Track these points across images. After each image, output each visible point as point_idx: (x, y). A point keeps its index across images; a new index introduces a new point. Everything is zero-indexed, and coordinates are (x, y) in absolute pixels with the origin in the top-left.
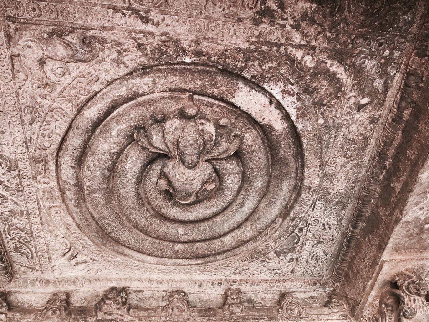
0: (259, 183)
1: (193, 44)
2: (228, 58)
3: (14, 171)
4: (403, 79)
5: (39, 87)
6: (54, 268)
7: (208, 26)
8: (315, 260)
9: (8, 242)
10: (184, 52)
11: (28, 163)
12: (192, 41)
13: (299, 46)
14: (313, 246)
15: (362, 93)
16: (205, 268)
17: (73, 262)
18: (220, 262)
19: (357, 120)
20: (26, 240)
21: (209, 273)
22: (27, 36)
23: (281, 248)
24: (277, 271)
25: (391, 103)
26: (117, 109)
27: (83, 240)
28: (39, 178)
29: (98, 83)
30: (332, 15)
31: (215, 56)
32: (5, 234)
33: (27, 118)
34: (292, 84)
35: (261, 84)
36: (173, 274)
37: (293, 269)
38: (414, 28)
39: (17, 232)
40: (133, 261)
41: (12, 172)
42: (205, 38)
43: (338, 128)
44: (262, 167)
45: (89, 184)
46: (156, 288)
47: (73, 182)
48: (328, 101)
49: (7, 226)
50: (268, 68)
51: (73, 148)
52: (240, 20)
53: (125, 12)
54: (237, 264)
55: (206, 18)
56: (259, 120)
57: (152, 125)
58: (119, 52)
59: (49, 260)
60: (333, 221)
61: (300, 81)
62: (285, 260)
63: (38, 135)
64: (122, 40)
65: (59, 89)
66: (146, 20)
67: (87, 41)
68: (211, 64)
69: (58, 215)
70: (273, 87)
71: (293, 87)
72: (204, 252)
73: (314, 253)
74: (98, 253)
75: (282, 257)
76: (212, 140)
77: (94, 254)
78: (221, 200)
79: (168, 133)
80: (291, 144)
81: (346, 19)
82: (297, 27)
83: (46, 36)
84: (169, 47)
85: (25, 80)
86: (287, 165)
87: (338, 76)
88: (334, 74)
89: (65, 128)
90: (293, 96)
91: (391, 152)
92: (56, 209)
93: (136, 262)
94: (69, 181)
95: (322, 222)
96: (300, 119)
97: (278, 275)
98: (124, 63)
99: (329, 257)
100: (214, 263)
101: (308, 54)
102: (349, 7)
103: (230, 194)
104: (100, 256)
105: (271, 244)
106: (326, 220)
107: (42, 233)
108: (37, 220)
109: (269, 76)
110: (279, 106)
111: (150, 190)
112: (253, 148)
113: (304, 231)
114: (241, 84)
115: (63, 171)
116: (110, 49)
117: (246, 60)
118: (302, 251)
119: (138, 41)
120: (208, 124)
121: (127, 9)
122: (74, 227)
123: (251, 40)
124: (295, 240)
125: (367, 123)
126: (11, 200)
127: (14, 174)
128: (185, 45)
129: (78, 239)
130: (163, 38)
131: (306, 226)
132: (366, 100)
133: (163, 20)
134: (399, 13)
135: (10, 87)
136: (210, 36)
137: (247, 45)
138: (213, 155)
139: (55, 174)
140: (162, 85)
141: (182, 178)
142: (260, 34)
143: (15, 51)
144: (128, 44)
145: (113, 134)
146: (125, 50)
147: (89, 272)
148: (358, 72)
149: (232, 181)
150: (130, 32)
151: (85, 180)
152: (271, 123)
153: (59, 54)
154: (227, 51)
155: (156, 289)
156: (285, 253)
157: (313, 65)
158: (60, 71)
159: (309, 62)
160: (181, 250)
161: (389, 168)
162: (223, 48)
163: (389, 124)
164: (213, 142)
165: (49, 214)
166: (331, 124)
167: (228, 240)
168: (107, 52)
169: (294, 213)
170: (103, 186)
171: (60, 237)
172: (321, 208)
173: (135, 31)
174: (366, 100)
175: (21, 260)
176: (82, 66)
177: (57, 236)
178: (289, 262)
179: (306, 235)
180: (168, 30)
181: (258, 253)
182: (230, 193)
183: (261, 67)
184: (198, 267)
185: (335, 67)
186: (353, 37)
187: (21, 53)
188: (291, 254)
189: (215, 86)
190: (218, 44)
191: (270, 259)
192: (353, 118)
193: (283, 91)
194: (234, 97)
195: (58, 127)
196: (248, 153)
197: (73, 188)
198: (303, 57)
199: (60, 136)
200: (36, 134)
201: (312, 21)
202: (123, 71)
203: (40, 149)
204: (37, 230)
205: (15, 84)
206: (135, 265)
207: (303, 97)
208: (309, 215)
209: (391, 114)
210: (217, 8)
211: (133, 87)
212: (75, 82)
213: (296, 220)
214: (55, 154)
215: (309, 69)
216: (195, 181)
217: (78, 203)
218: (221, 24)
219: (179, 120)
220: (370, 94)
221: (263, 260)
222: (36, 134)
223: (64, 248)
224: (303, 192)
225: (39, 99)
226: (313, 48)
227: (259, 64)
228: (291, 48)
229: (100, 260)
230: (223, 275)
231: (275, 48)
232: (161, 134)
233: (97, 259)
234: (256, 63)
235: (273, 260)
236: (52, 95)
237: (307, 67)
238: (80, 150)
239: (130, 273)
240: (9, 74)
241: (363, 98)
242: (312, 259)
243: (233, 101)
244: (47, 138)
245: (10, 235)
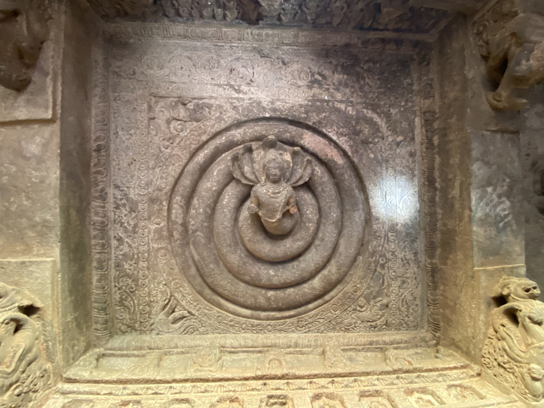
0: (334, 214)
1: (270, 104)
2: (295, 112)
3: (134, 212)
4: (421, 118)
5: (164, 140)
6: (152, 327)
7: (278, 92)
8: (405, 307)
9: (115, 292)
10: (264, 109)
11: (146, 205)
12: (269, 102)
13: (341, 102)
14: (399, 286)
15: (394, 131)
16: (298, 322)
17: (171, 317)
18: (313, 312)
19: (399, 153)
20: (131, 290)
21: (304, 328)
22: (162, 104)
23: (369, 291)
24: (372, 324)
25: (420, 138)
26: (219, 157)
27: (183, 287)
28: (152, 218)
29: (206, 135)
30: (358, 81)
31: (285, 112)
32: (115, 282)
33: (152, 163)
34: (343, 128)
35: (320, 129)
36: (267, 332)
37: (387, 321)
38: (415, 87)
39: (125, 279)
40: (228, 314)
41: (132, 213)
42: (278, 100)
43: (387, 161)
44: (334, 198)
45: (193, 222)
46: (252, 347)
47: (180, 221)
48: (373, 139)
49: (118, 273)
50: (323, 117)
51: (183, 188)
52: (299, 87)
53: (225, 87)
54: (330, 314)
55: (277, 87)
56: (323, 158)
57: (243, 154)
58: (221, 113)
59: (149, 315)
60: (410, 256)
61: (348, 125)
62: (376, 307)
63: (158, 178)
64: (223, 104)
65: (178, 140)
66: (238, 91)
67: (201, 106)
68: (283, 117)
69: (164, 258)
70: (330, 130)
71: (344, 130)
72: (295, 298)
73: (403, 297)
74: (195, 304)
75: (372, 303)
76: (290, 167)
77: (191, 306)
78: (304, 233)
79: (255, 162)
80: (353, 177)
81: (368, 84)
82: (337, 89)
83: (173, 104)
84: (254, 107)
85: (156, 135)
86: (354, 196)
87: (375, 120)
88: (371, 119)
89: (179, 171)
90: (345, 136)
92: (163, 251)
93: (230, 315)
94: (177, 220)
95: (400, 256)
96: (355, 154)
97: (373, 329)
98: (224, 120)
99: (418, 302)
100: (306, 314)
101: (349, 106)
102: (368, 76)
103: (312, 227)
104: (197, 308)
105: (358, 286)
106: (403, 255)
107: (147, 281)
108: (144, 265)
109: (325, 122)
110: (337, 145)
111: (243, 225)
112: (323, 179)
113: (386, 268)
114: (306, 131)
115: (174, 211)
116: (214, 111)
117: (306, 113)
118: (389, 294)
119: (234, 104)
120: (285, 153)
121: (226, 85)
122: (177, 270)
123: (308, 99)
124: (380, 280)
125: (407, 156)
126: (127, 242)
127: (134, 215)
128: (265, 104)
129: (178, 286)
130: (250, 101)
131: (386, 262)
132: (400, 138)
133: (249, 90)
134: (402, 79)
135: (143, 141)
136: (281, 98)
137: (306, 102)
138: (292, 182)
139: (166, 214)
140: (250, 134)
141: (268, 192)
142: (314, 94)
143: (152, 115)
144: (227, 106)
145: (215, 174)
146: (225, 111)
147: (185, 332)
148: (388, 117)
149: (311, 212)
150: (228, 99)
151: (191, 220)
152: (334, 158)
153: (181, 115)
154: (293, 107)
155: (251, 349)
156: (375, 298)
157: (354, 113)
158: (180, 127)
159: (351, 111)
160: (273, 296)
161: (441, 187)
162: (290, 105)
163: (425, 153)
164: (290, 169)
165: (156, 257)
166: (380, 157)
167: (317, 283)
168: (212, 113)
169: (371, 246)
170: (206, 224)
171: (162, 285)
172: (395, 241)
173: (232, 98)
174: (400, 138)
175: (124, 316)
176: (195, 124)
177: (159, 283)
178: (381, 310)
179: (389, 273)
180: (253, 96)
181: (348, 299)
182: (310, 225)
183: (318, 116)
184: (291, 320)
185: (369, 114)
186: (376, 94)
187: (156, 116)
188: (380, 299)
189: (287, 131)
190: (286, 103)
191: (362, 307)
192: (396, 152)
193: (337, 132)
194: (302, 139)
195: (174, 170)
196: (320, 185)
197: (180, 228)
198: (346, 108)
199: (174, 177)
200: (156, 177)
201: (346, 85)
202: (223, 126)
203: (157, 190)
204: (143, 276)
205: (148, 138)
206: (230, 319)
207: (353, 136)
208: (386, 249)
209: (424, 145)
210: (284, 81)
211: (229, 136)
212: (189, 135)
213: (376, 254)
214: (169, 194)
215: (352, 116)
216: (279, 195)
217: (183, 244)
218: (287, 90)
219: (263, 150)
220: (402, 133)
221: (355, 307)
222: (156, 177)
223: (164, 298)
224: (374, 223)
225: (163, 149)
226: (351, 102)
227: (316, 114)
228: (336, 103)
229: (197, 314)
230: (318, 332)
231: (326, 104)
232: (250, 165)
233: (193, 312)
234: (314, 114)
235: (364, 309)
236: (173, 145)
237: (351, 115)
238: (188, 189)
239: (224, 332)
240: (145, 132)
241: (398, 136)
242: (403, 306)
243: (302, 142)
244: (164, 180)
245: (119, 284)
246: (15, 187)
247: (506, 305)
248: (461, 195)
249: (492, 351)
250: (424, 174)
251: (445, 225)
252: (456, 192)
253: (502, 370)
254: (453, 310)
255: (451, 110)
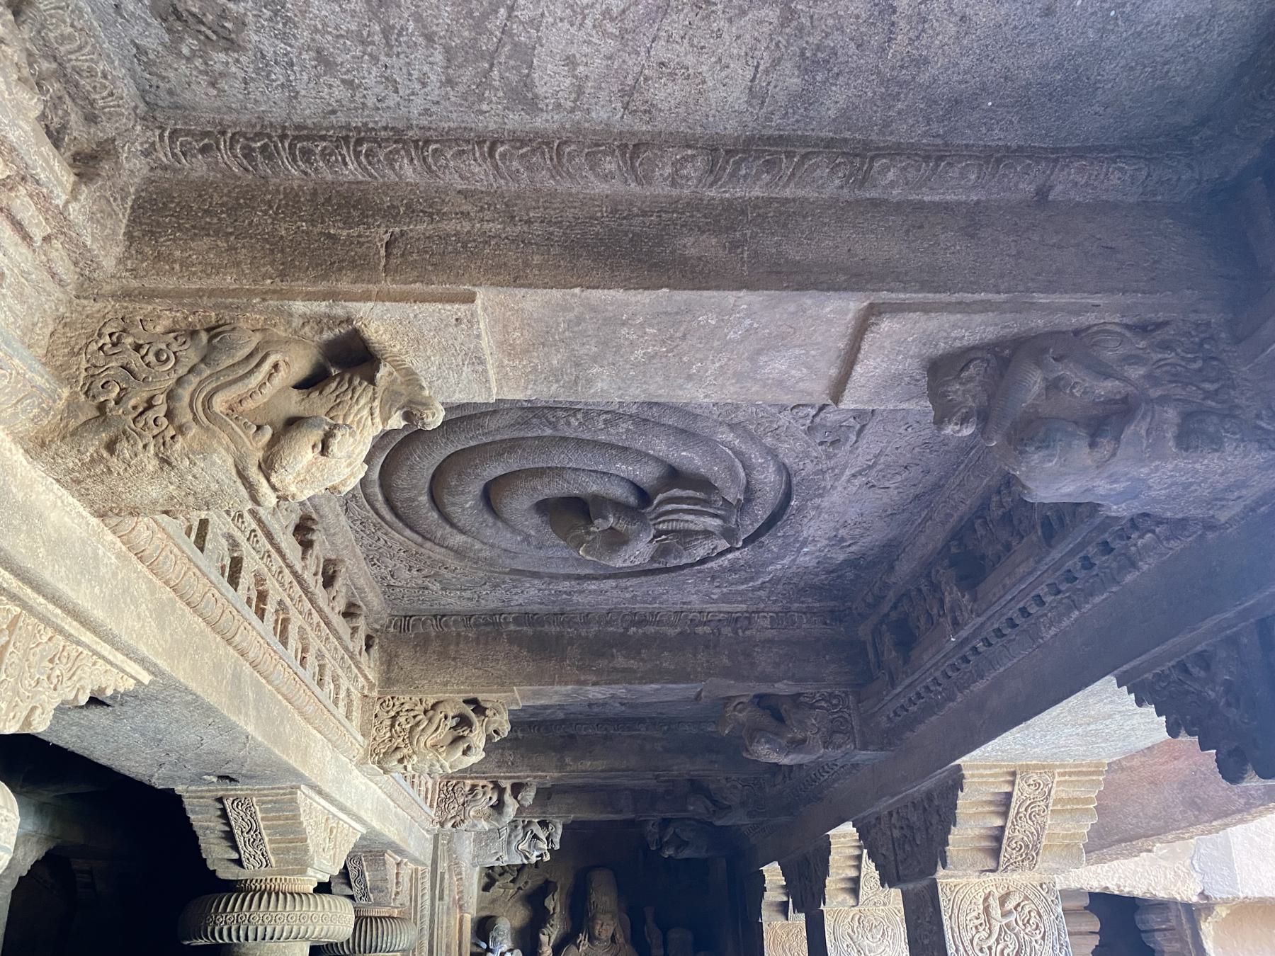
4: (742, 613)
91: (651, 629)
246: (684, 337)
247: (473, 715)
248: (616, 670)
249: (407, 707)
250: (652, 614)
251: (571, 641)
252: (620, 661)
253: (388, 722)
254: (443, 655)
255: (741, 658)
